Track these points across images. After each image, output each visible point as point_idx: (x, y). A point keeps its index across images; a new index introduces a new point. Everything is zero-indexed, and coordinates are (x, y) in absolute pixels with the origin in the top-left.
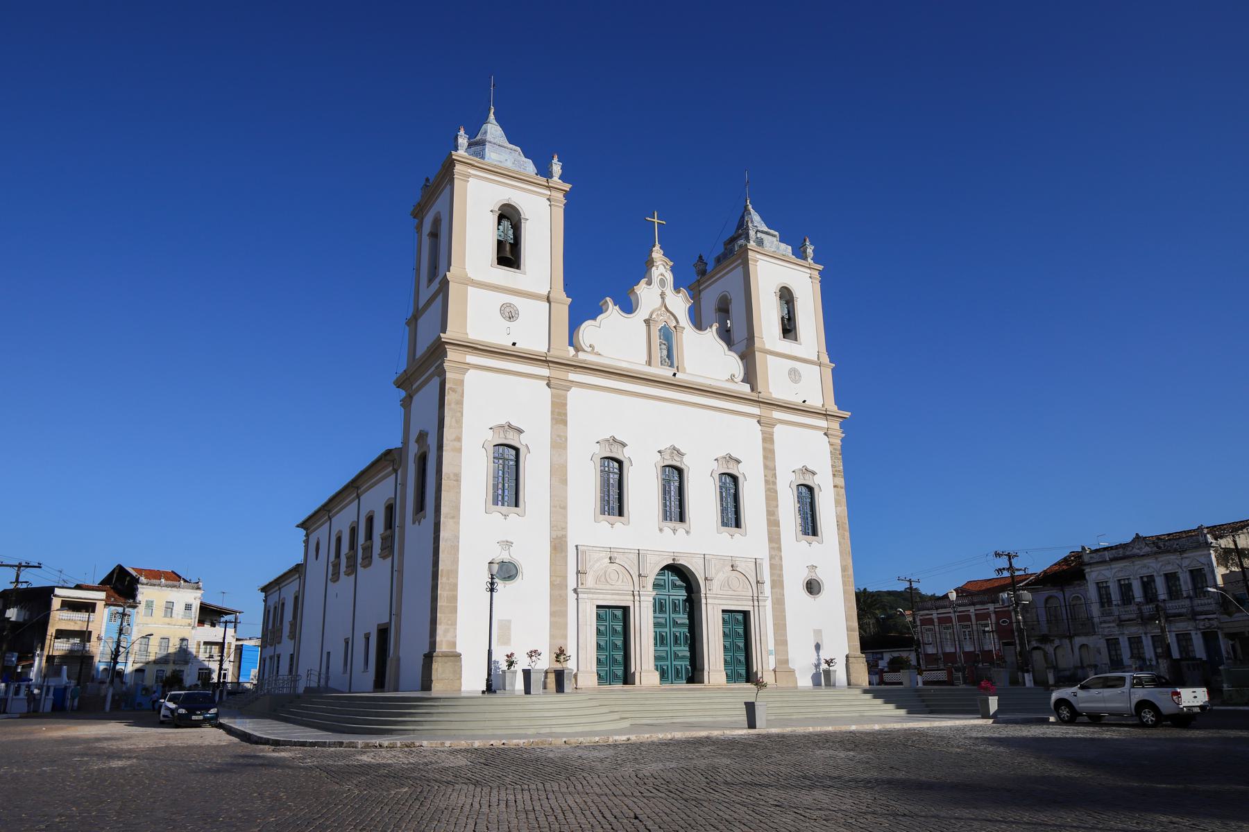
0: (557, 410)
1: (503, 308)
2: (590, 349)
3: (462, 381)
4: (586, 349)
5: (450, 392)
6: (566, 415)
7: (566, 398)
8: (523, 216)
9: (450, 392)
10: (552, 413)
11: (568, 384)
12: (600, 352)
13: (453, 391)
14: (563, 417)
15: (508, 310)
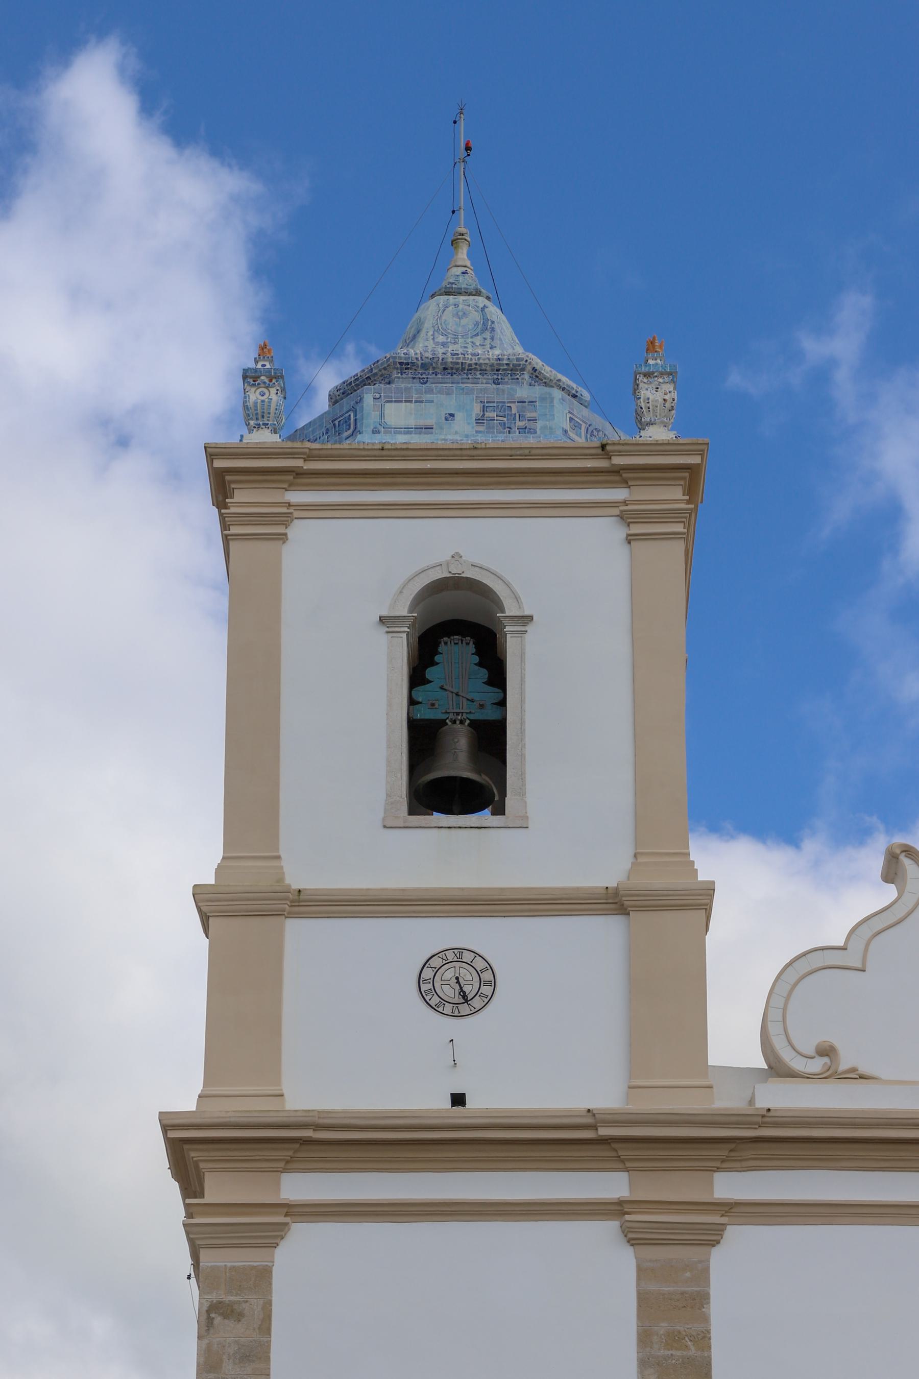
0: (662, 1327)
1: (428, 973)
2: (817, 1065)
3: (264, 1275)
4: (798, 1064)
5: (218, 1320)
6: (703, 1340)
7: (703, 1274)
8: (511, 609)
9: (218, 1320)
10: (644, 1338)
11: (717, 1219)
12: (864, 1069)
13: (225, 1316)
14: (693, 1351)
15: (449, 974)
